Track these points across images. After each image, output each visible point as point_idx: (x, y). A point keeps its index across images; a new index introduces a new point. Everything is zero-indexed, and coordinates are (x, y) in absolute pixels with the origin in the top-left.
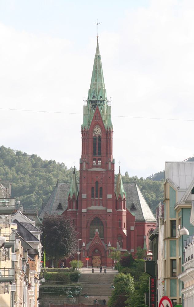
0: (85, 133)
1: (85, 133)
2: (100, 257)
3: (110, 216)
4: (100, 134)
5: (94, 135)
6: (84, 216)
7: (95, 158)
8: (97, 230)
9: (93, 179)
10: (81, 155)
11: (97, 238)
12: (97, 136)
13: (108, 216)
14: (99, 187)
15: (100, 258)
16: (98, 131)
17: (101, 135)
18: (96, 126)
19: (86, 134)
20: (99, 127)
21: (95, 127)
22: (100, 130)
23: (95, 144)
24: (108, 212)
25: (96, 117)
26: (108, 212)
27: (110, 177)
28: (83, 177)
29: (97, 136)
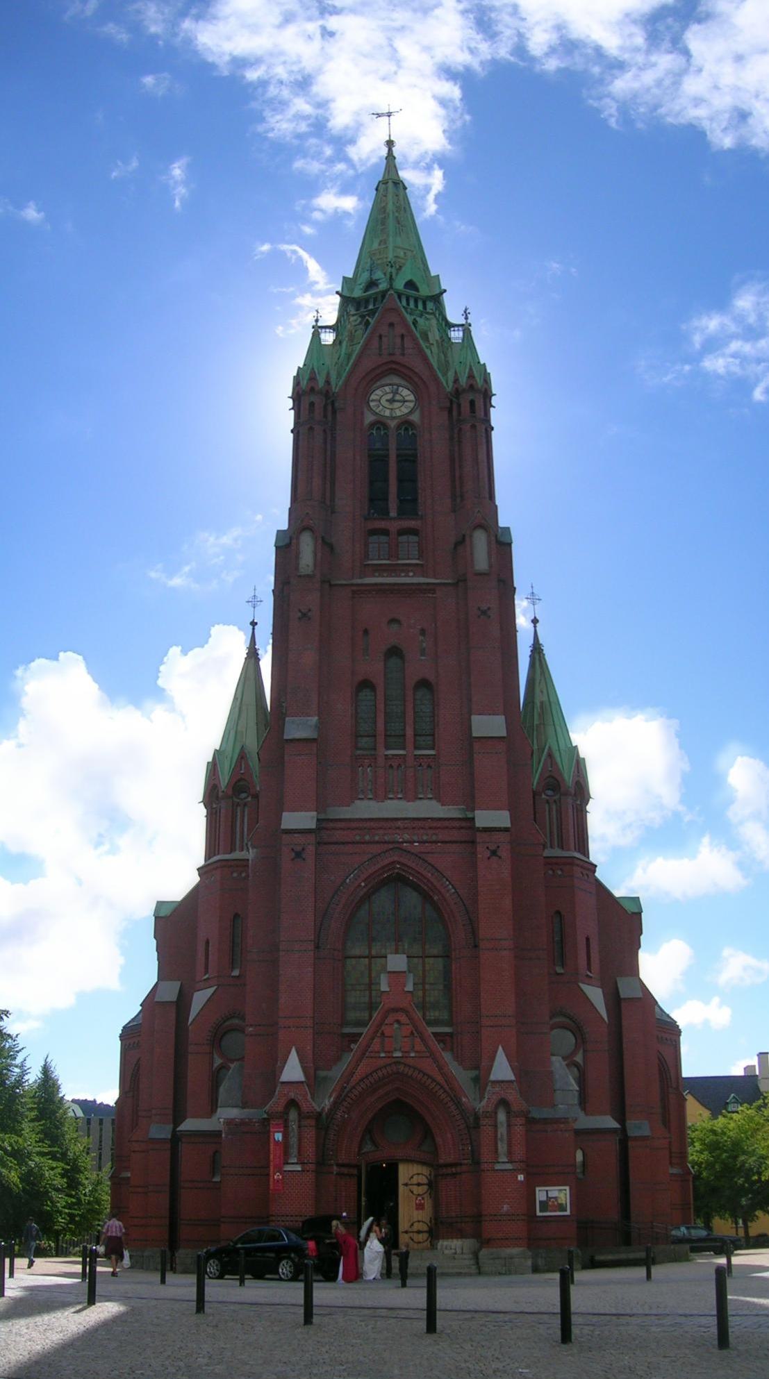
2: (425, 1170)
3: (494, 853)
4: (411, 412)
5: (369, 418)
6: (298, 855)
7: (382, 524)
8: (397, 962)
9: (366, 632)
12: (393, 424)
13: (482, 852)
15: (425, 1181)
16: (392, 402)
17: (415, 418)
18: (387, 380)
20: (403, 382)
21: (378, 384)
22: (412, 397)
24: (478, 824)
25: (384, 339)
26: (478, 824)
29: (393, 424)
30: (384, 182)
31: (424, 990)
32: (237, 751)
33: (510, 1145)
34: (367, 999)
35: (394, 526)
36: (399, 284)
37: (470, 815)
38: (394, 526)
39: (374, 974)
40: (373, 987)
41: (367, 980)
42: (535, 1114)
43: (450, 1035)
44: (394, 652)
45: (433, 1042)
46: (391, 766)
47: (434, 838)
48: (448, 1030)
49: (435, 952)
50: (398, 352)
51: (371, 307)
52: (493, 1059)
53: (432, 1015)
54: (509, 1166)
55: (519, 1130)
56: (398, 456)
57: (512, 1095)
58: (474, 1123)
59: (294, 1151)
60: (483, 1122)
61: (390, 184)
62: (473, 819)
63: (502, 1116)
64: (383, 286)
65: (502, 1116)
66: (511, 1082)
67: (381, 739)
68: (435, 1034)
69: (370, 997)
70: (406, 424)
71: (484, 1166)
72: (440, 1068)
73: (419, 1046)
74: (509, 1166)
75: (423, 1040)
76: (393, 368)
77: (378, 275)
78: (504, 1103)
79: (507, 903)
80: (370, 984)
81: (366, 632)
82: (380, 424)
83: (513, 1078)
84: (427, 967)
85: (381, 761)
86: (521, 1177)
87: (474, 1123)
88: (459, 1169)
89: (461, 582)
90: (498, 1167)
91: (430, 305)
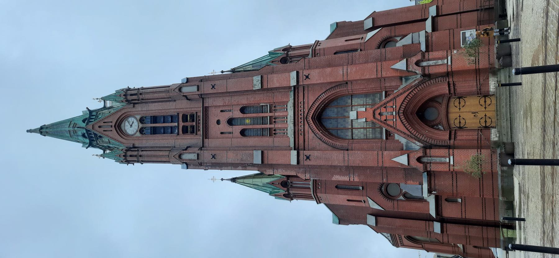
0: (131, 156)
1: (131, 156)
3: (307, 77)
5: (138, 134)
6: (308, 158)
8: (353, 115)
10: (171, 165)
11: (378, 112)
12: (141, 125)
14: (241, 115)
17: (138, 117)
19: (131, 155)
23: (154, 131)
24: (295, 84)
26: (295, 84)
27: (213, 87)
28: (214, 161)
29: (141, 125)
30: (41, 133)
31: (366, 105)
32: (270, 186)
33: (439, 59)
34: (371, 129)
35: (182, 124)
36: (84, 125)
37: (293, 88)
38: (182, 124)
39: (359, 127)
40: (365, 127)
41: (362, 130)
42: (423, 48)
43: (386, 92)
44: (230, 122)
45: (389, 98)
46: (275, 122)
47: (302, 103)
48: (384, 93)
49: (350, 101)
50: (111, 124)
51: (93, 136)
52: (397, 70)
53: (377, 100)
54: (449, 58)
55: (432, 55)
56: (154, 123)
57: (414, 59)
58: (427, 76)
59: (443, 160)
60: (427, 72)
61: (42, 130)
62: (294, 87)
63: (424, 64)
64: (85, 132)
65: (424, 64)
66: (407, 60)
67: (264, 126)
68: (386, 97)
69: (369, 128)
70: (142, 120)
71: (450, 70)
72: (401, 94)
73: (391, 104)
74: (449, 58)
75: (388, 102)
76: (118, 126)
77: (80, 133)
78: (417, 64)
79: (328, 70)
80: (364, 128)
81: (222, 133)
82: (141, 131)
83: (405, 59)
84: (356, 104)
85: (272, 126)
86: (455, 52)
87: (427, 76)
88: (451, 83)
89: (202, 97)
90: (449, 63)
91: (94, 113)
